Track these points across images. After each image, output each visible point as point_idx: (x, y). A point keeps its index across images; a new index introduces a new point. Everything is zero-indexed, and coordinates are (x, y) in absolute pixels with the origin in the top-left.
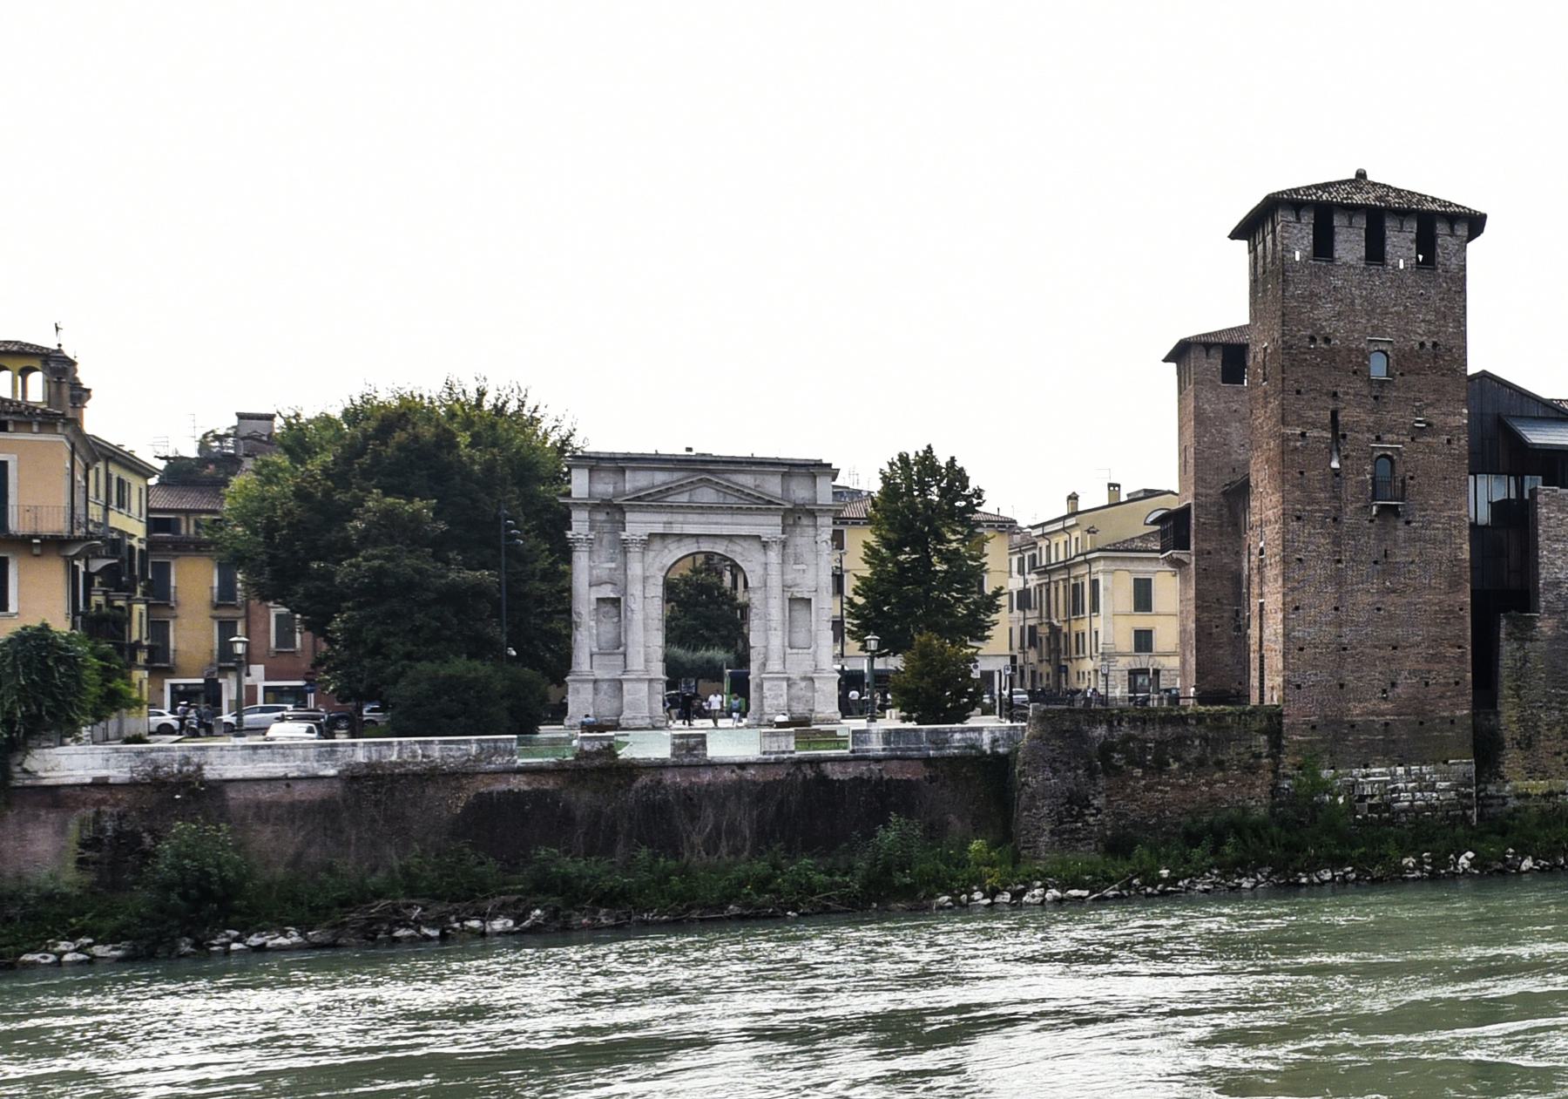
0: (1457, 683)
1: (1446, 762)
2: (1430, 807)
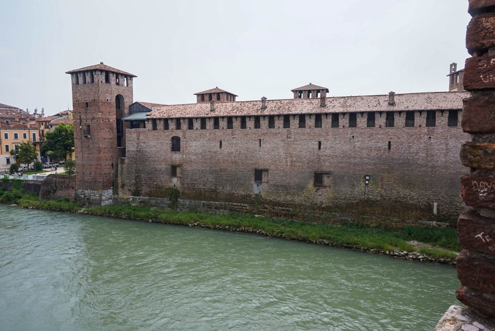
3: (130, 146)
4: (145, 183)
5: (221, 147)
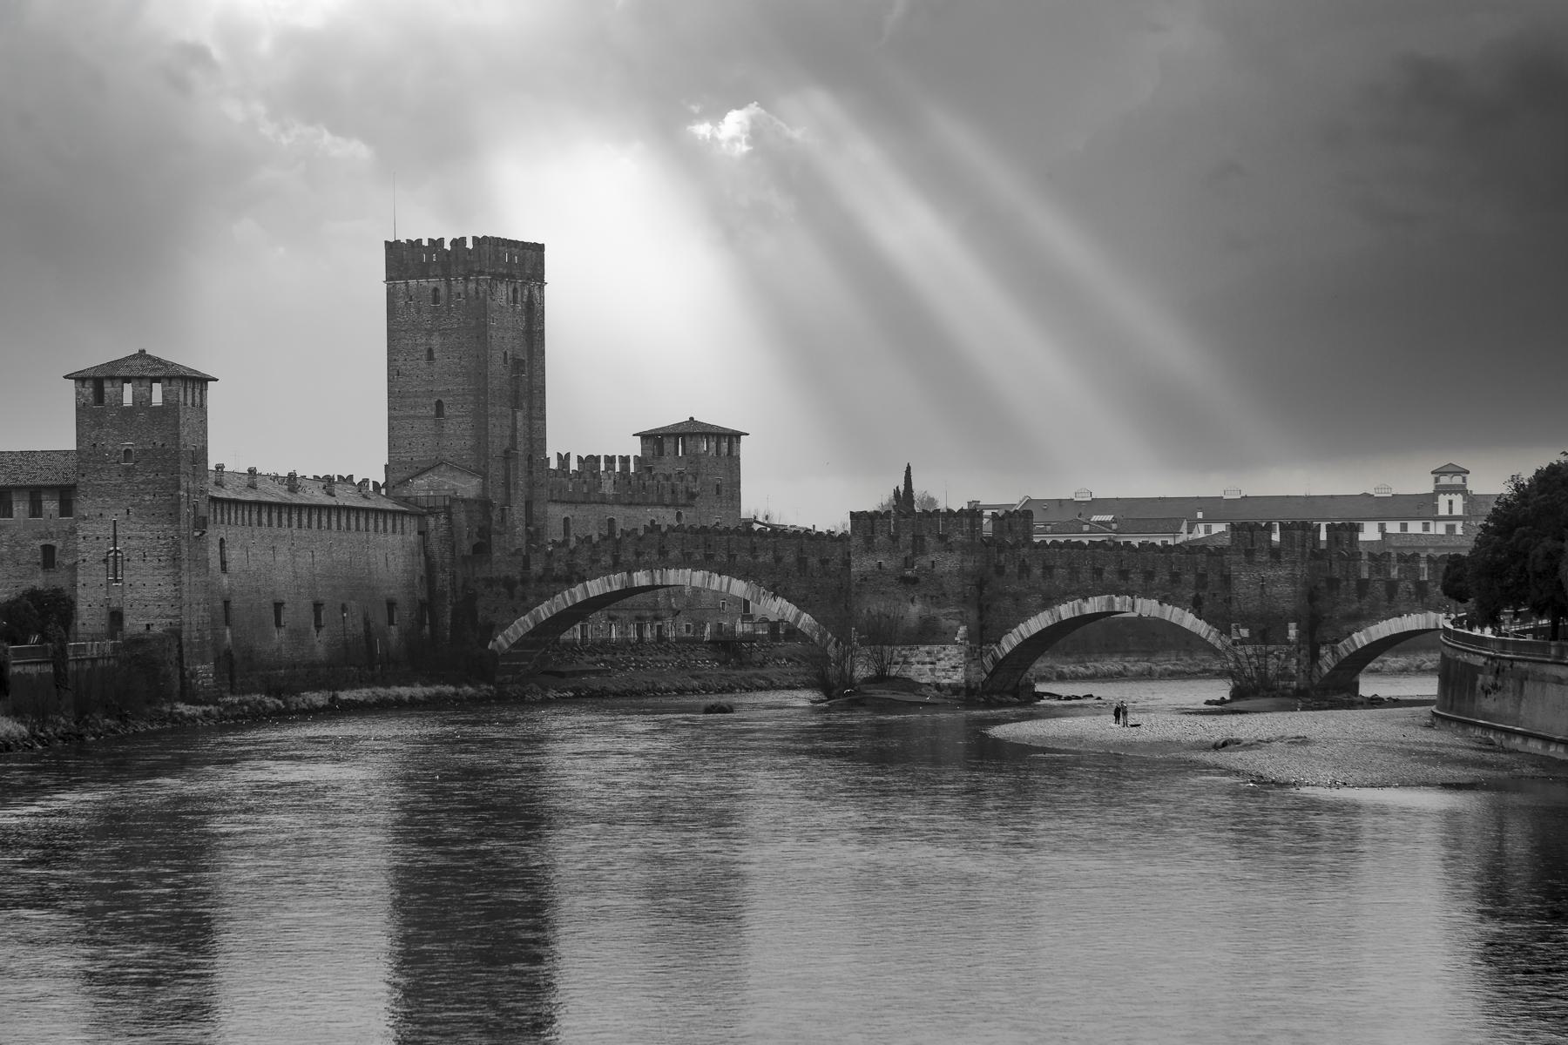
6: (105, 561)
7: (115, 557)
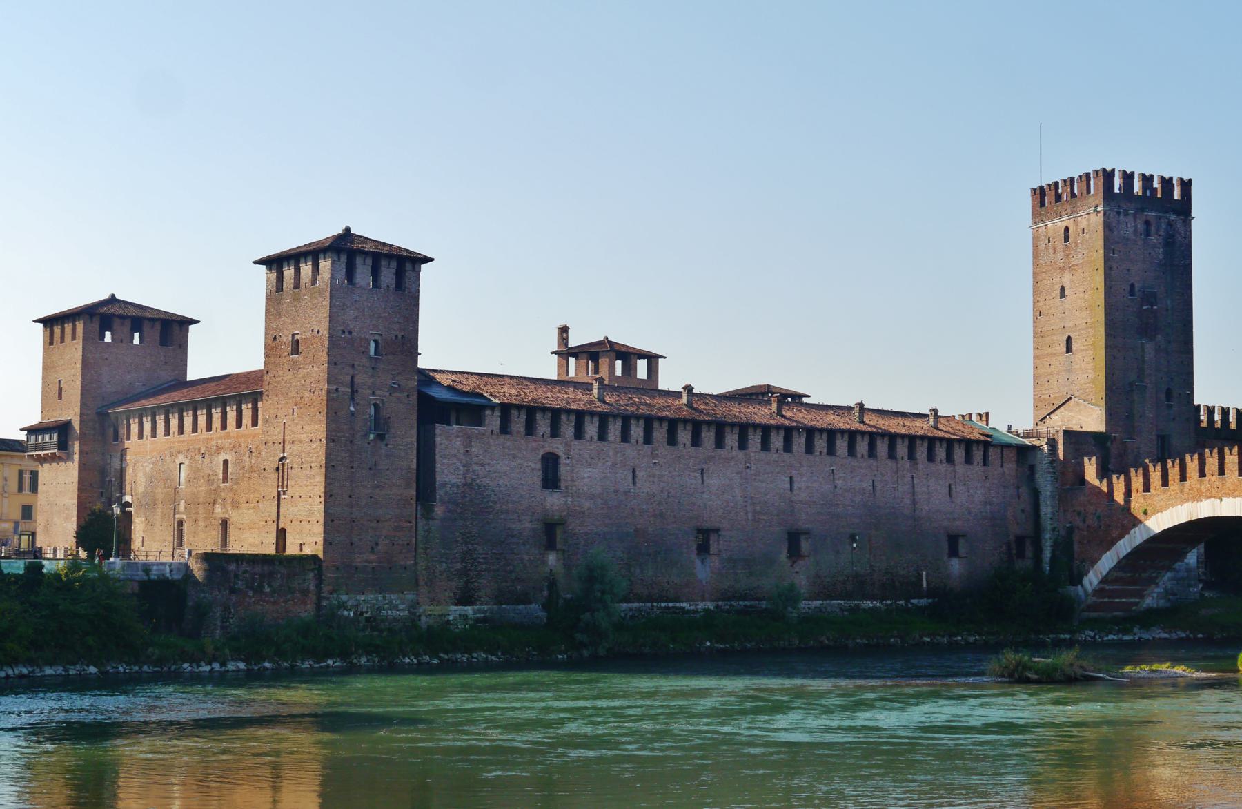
0: (408, 544)
1: (403, 593)
2: (395, 620)
3: (446, 471)
4: (485, 570)
5: (634, 483)
6: (277, 469)
7: (283, 464)
